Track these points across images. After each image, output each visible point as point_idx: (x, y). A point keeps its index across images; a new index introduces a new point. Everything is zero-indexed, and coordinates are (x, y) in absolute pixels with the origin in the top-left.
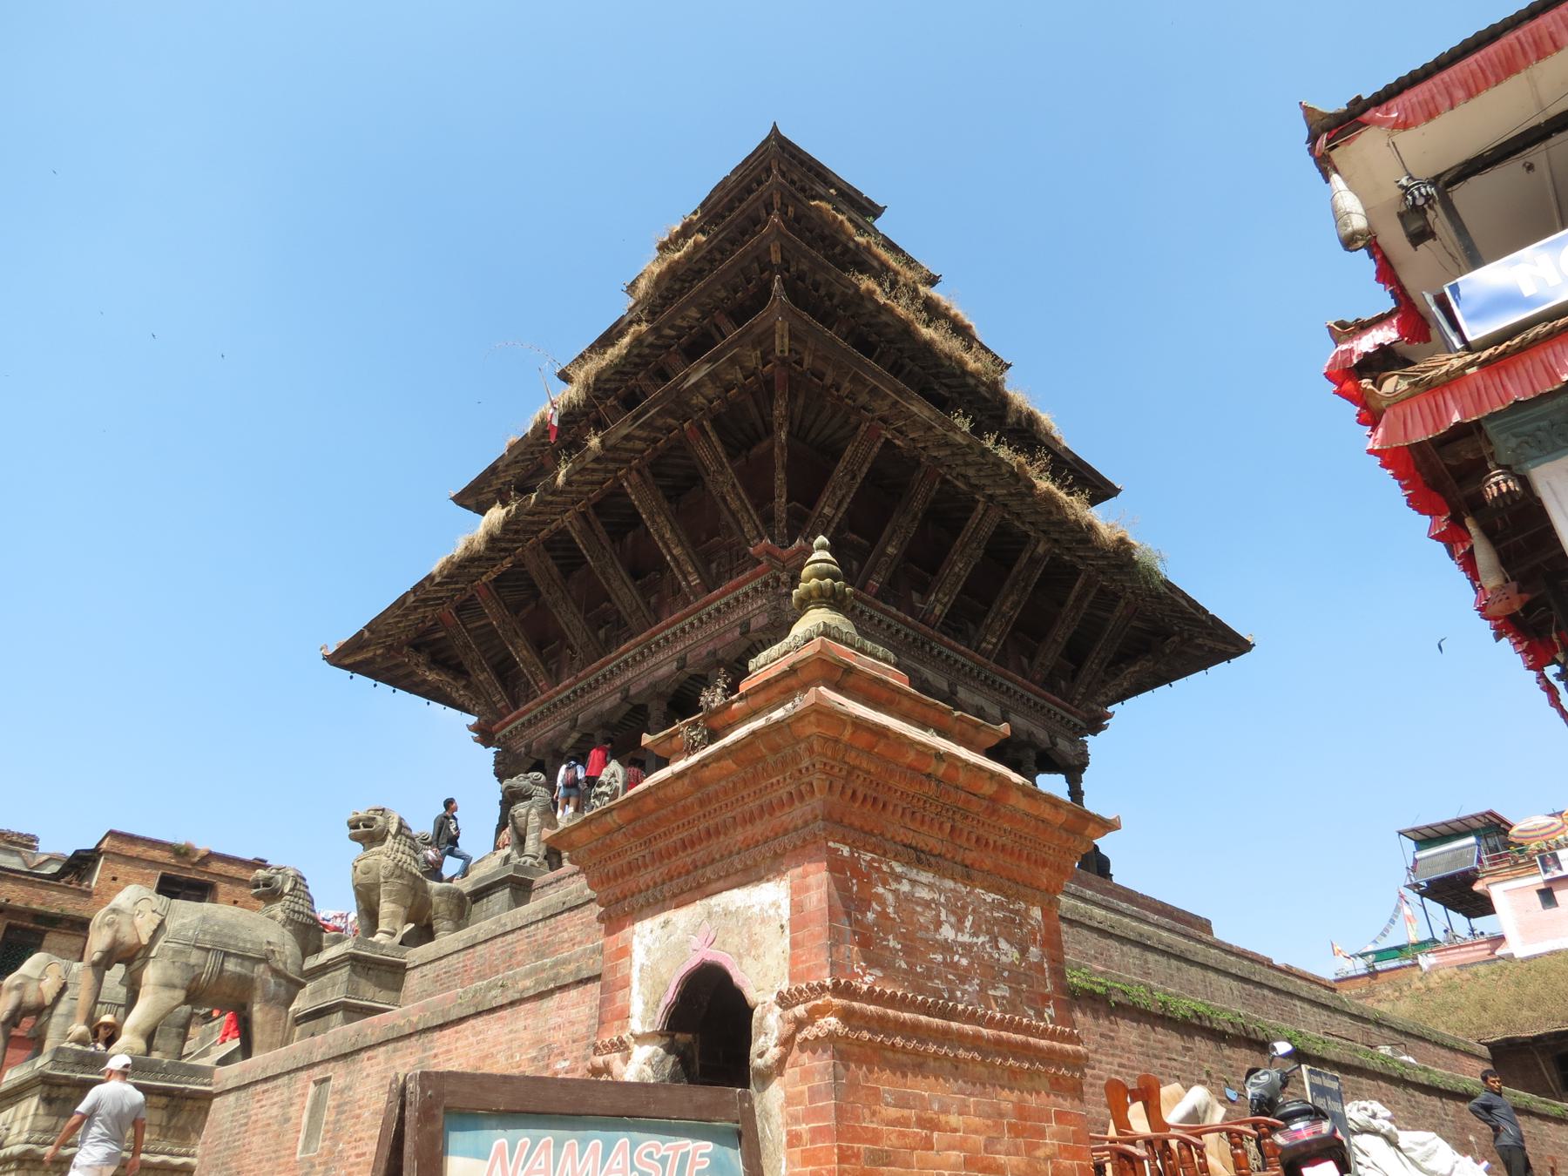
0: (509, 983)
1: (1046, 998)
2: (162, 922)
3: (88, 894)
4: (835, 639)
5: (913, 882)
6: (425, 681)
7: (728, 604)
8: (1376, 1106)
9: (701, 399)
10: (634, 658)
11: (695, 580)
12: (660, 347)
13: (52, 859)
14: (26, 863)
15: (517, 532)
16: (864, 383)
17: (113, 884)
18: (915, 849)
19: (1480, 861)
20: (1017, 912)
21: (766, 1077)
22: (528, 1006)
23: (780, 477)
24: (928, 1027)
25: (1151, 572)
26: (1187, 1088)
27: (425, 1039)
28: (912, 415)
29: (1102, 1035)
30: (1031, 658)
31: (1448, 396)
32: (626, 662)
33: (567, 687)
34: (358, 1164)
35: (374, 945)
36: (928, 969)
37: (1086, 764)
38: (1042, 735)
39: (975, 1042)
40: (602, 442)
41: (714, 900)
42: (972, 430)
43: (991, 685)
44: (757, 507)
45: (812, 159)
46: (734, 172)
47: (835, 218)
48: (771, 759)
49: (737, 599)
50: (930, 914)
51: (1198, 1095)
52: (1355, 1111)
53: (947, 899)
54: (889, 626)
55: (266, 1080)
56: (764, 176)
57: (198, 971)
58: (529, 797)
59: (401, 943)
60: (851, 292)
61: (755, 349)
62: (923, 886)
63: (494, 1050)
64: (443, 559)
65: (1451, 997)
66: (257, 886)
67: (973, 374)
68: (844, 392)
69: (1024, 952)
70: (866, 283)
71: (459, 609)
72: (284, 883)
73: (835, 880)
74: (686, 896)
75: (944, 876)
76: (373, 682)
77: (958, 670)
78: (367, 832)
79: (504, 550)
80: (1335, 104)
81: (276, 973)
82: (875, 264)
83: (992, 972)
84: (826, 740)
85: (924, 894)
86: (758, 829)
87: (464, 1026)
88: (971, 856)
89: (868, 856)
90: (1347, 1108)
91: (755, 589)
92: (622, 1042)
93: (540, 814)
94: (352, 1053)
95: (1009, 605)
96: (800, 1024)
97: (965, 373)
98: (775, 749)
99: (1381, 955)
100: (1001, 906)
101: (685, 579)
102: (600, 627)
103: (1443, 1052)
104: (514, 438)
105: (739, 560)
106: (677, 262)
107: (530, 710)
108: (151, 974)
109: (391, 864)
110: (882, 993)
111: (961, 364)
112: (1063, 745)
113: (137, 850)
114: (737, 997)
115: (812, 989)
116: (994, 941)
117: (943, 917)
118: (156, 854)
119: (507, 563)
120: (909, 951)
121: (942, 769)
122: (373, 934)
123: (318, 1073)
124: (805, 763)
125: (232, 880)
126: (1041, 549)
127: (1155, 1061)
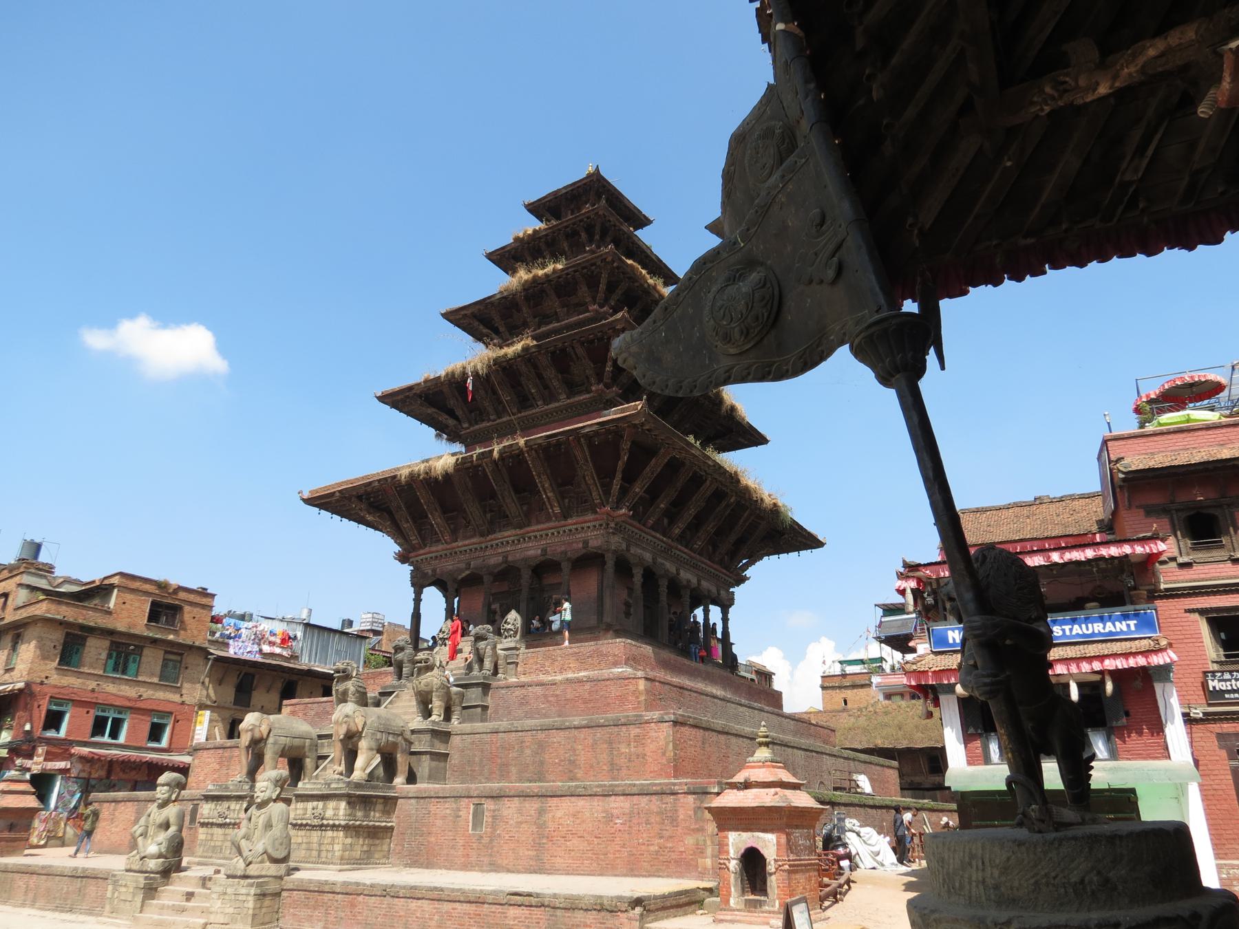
3: (109, 613)
8: (855, 821)
11: (557, 510)
21: (771, 874)
23: (619, 476)
27: (543, 799)
28: (687, 451)
35: (434, 722)
38: (714, 590)
39: (805, 865)
43: (695, 567)
62: (797, 833)
81: (406, 740)
83: (805, 847)
95: (710, 527)
105: (582, 504)
108: (363, 744)
113: (137, 585)
118: (147, 587)
123: (476, 801)
125: (191, 604)
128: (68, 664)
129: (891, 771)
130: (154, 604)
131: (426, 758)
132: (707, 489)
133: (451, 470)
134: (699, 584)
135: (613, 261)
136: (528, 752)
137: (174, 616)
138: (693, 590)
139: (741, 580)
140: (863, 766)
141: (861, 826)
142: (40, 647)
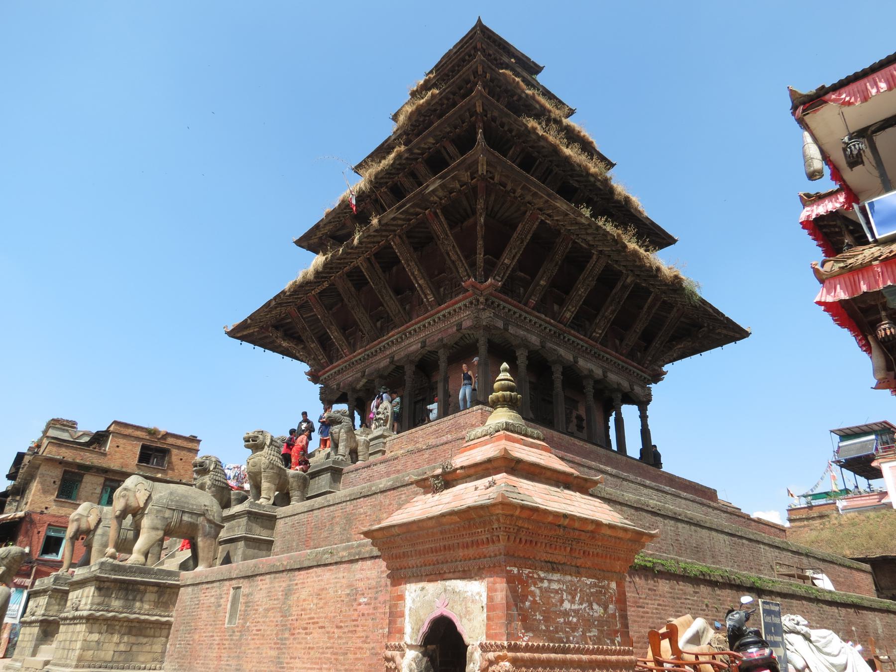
0: (335, 552)
1: (616, 632)
2: (150, 495)
3: (105, 455)
4: (512, 432)
5: (550, 581)
6: (280, 345)
7: (449, 313)
8: (799, 618)
9: (436, 198)
10: (397, 340)
11: (431, 298)
12: (412, 159)
13: (85, 434)
14: (71, 436)
15: (331, 268)
16: (529, 190)
17: (117, 449)
18: (551, 563)
19: (877, 449)
20: (603, 587)
22: (345, 566)
23: (480, 243)
24: (555, 660)
25: (693, 293)
26: (694, 618)
27: (290, 574)
28: (556, 208)
29: (649, 589)
30: (621, 340)
31: (861, 276)
32: (392, 342)
33: (359, 354)
34: (257, 635)
35: (260, 505)
36: (556, 628)
37: (650, 400)
38: (625, 384)
39: (579, 664)
40: (379, 221)
41: (448, 583)
42: (592, 216)
43: (597, 356)
44: (466, 258)
45: (501, 39)
46: (455, 47)
47: (514, 80)
48: (477, 520)
49: (455, 310)
50: (558, 597)
51: (699, 623)
52: (787, 621)
53: (567, 587)
54: (540, 325)
55: (207, 583)
56: (472, 52)
57: (169, 521)
58: (341, 423)
59: (274, 504)
60: (523, 129)
61: (466, 171)
62: (555, 582)
63: (327, 587)
64: (291, 282)
65: (853, 530)
66: (196, 466)
67: (592, 175)
68: (517, 194)
69: (606, 608)
70: (532, 123)
71: (300, 308)
72: (210, 465)
73: (510, 588)
74: (433, 577)
75: (566, 574)
76: (252, 346)
77: (579, 349)
78: (254, 444)
79: (326, 277)
80: (808, 88)
81: (209, 521)
82: (538, 106)
83: (588, 622)
84: (507, 516)
85: (555, 586)
86: (471, 552)
87: (311, 571)
88: (579, 562)
89: (527, 571)
90: (783, 618)
91: (465, 305)
92: (400, 647)
93: (346, 432)
94: (252, 576)
95: (609, 312)
96: (491, 663)
97: (588, 174)
98: (481, 517)
99: (816, 496)
100: (595, 585)
101: (426, 297)
102: (378, 320)
103: (844, 569)
104: (329, 209)
105: (456, 288)
106: (422, 105)
107: (339, 365)
108: (146, 522)
109: (267, 462)
110: (533, 645)
111: (586, 169)
112: (637, 389)
113: (129, 431)
114: (459, 637)
115: (497, 646)
116: (591, 605)
117: (565, 597)
118: (139, 433)
119: (326, 285)
120: (547, 619)
121: (566, 522)
122: (258, 498)
123: (234, 583)
124: (496, 526)
125: (179, 448)
126: (629, 280)
127: (677, 601)
128: (69, 497)
129: (863, 575)
130: (144, 447)
131: (241, 544)
132: (595, 266)
133: (320, 269)
134: (605, 376)
135: (485, 72)
136: (337, 529)
137: (163, 458)
138: (597, 382)
139: (657, 377)
140: (822, 565)
141: (811, 627)
142: (42, 483)
